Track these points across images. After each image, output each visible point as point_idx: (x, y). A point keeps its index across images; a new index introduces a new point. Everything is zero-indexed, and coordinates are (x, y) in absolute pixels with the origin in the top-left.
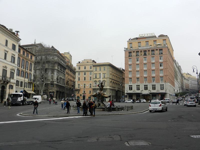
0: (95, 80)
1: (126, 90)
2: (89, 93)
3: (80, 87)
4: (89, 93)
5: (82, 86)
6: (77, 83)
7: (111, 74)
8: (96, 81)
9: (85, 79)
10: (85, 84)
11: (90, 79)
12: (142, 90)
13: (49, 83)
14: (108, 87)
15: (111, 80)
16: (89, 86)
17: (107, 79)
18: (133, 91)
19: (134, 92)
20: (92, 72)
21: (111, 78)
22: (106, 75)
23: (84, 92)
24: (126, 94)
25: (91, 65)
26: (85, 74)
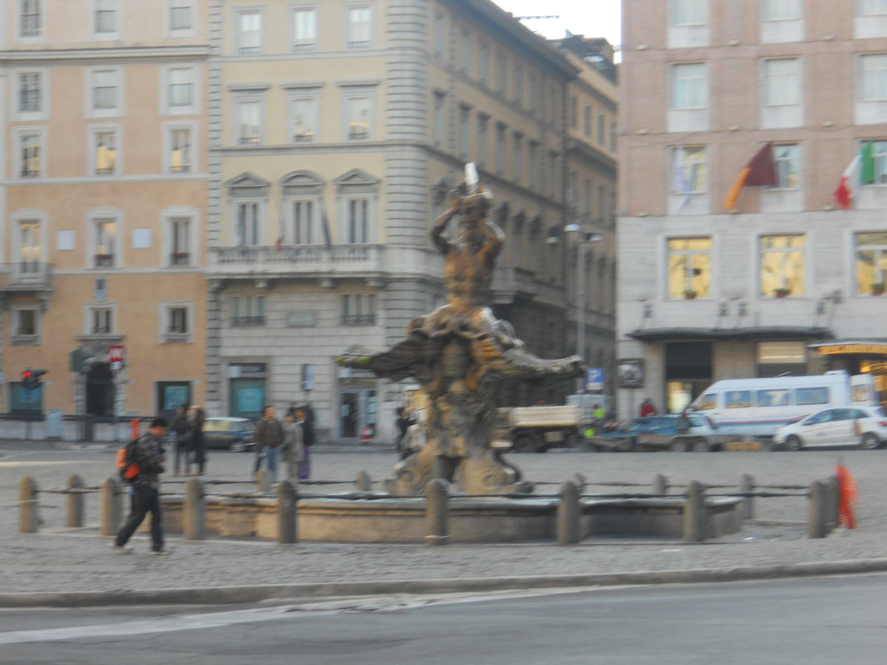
0: (234, 167)
1: (637, 290)
2: (171, 341)
4: (171, 341)
7: (439, 95)
12: (836, 298)
14: (407, 263)
16: (156, 239)
18: (723, 313)
19: (728, 324)
21: (444, 148)
23: (103, 319)
24: (627, 349)
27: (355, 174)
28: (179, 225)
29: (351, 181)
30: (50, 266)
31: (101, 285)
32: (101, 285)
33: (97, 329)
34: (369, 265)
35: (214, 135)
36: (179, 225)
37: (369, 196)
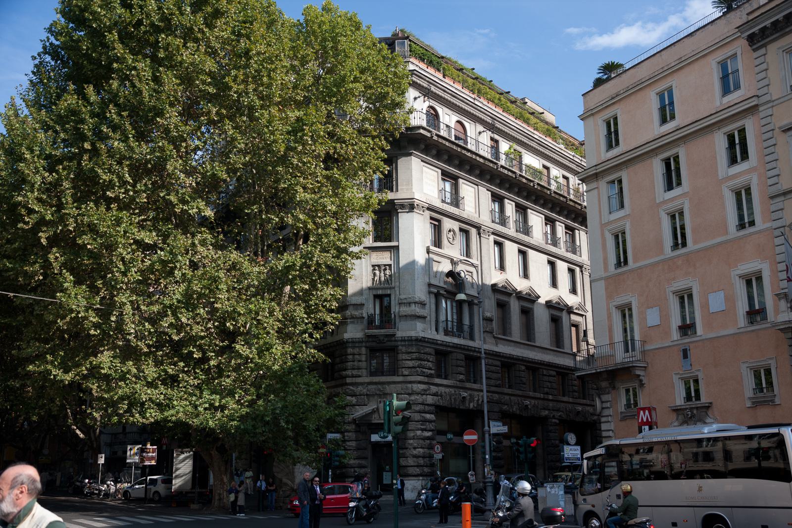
3: (637, 337)
5: (653, 318)
6: (609, 297)
9: (679, 239)
10: (685, 297)
11: (732, 219)
13: (354, 342)
16: (730, 300)
25: (723, 44)
26: (672, 175)
28: (752, 281)
30: (644, 342)
31: (685, 354)
32: (685, 354)
33: (688, 398)
35: (770, 182)
36: (752, 281)
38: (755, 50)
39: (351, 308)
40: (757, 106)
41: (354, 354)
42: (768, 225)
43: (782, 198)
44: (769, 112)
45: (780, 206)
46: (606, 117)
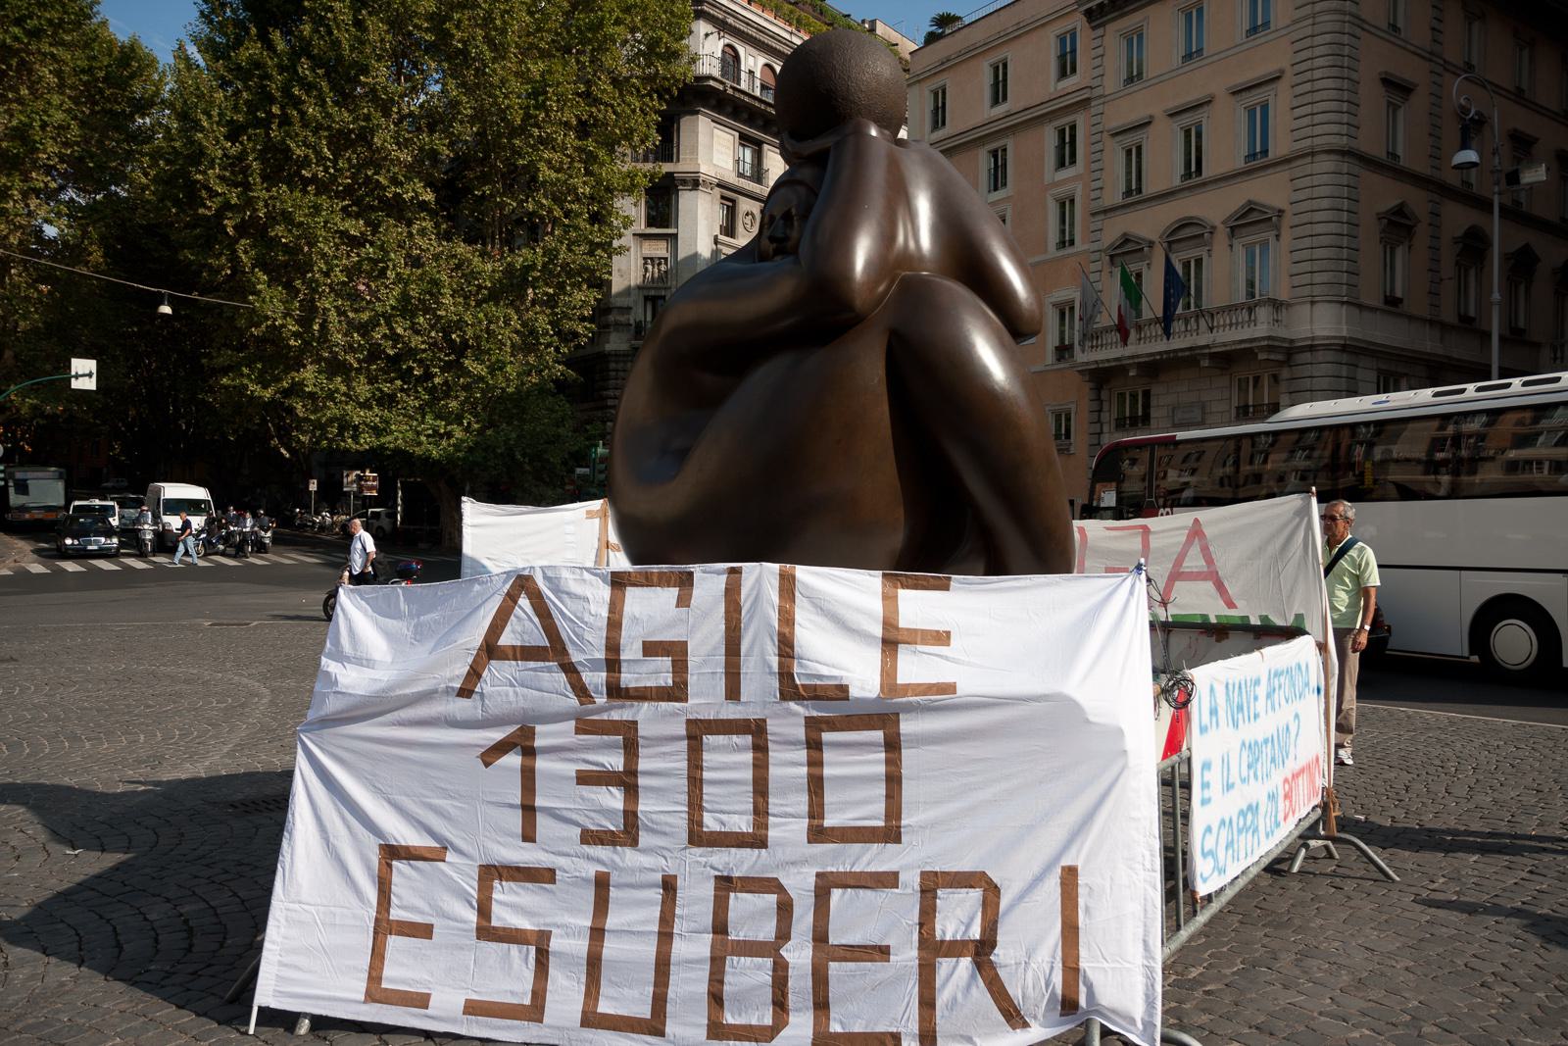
0: (1114, 229)
8: (1127, 249)
11: (1053, 237)
15: (1386, 194)
17: (1305, 167)
20: (1081, 120)
22: (1281, 100)
27: (1250, 208)
29: (1250, 219)
34: (1262, 327)
35: (1094, 195)
37: (1270, 235)
38: (1094, 28)
39: (615, 312)
40: (1088, 100)
41: (617, 371)
42: (1086, 247)
43: (1102, 217)
44: (1100, 109)
45: (1099, 225)
46: (934, 87)
